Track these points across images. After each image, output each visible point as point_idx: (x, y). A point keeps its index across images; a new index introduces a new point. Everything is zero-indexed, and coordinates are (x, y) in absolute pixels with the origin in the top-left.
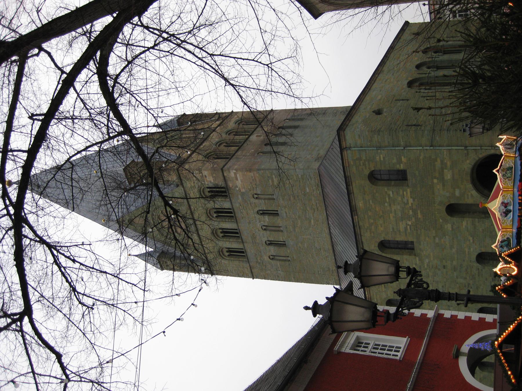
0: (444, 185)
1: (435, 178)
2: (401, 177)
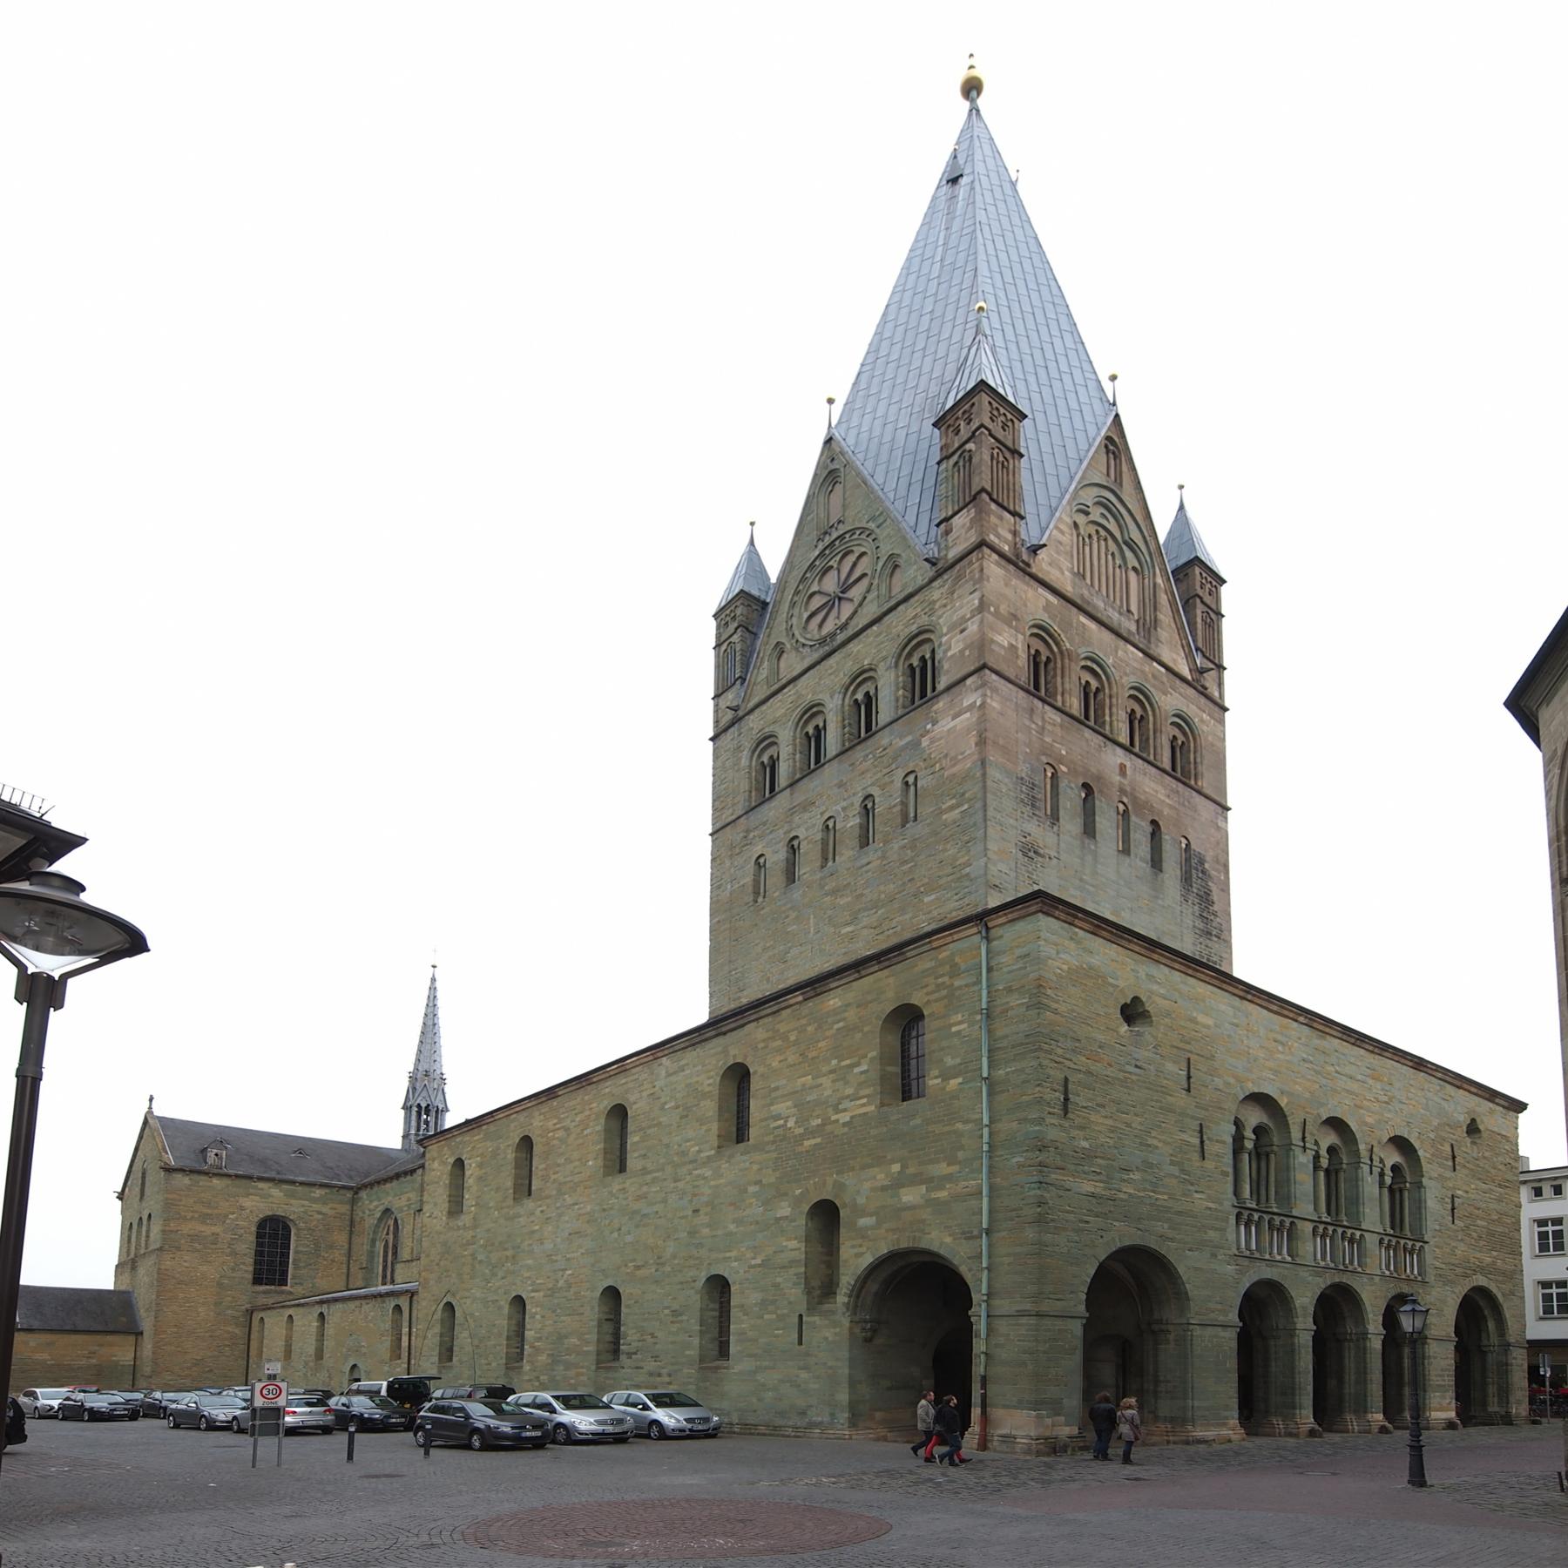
0: (884, 1188)
1: (904, 1167)
2: (905, 1082)
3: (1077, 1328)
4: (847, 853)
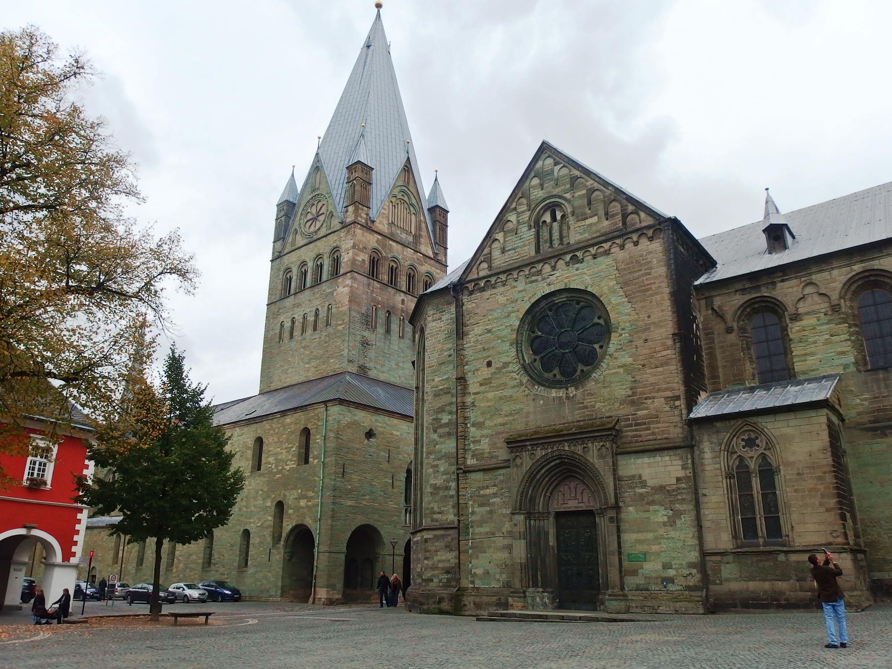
0: (296, 499)
3: (343, 557)
4: (309, 331)
